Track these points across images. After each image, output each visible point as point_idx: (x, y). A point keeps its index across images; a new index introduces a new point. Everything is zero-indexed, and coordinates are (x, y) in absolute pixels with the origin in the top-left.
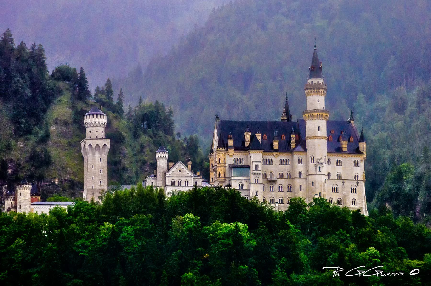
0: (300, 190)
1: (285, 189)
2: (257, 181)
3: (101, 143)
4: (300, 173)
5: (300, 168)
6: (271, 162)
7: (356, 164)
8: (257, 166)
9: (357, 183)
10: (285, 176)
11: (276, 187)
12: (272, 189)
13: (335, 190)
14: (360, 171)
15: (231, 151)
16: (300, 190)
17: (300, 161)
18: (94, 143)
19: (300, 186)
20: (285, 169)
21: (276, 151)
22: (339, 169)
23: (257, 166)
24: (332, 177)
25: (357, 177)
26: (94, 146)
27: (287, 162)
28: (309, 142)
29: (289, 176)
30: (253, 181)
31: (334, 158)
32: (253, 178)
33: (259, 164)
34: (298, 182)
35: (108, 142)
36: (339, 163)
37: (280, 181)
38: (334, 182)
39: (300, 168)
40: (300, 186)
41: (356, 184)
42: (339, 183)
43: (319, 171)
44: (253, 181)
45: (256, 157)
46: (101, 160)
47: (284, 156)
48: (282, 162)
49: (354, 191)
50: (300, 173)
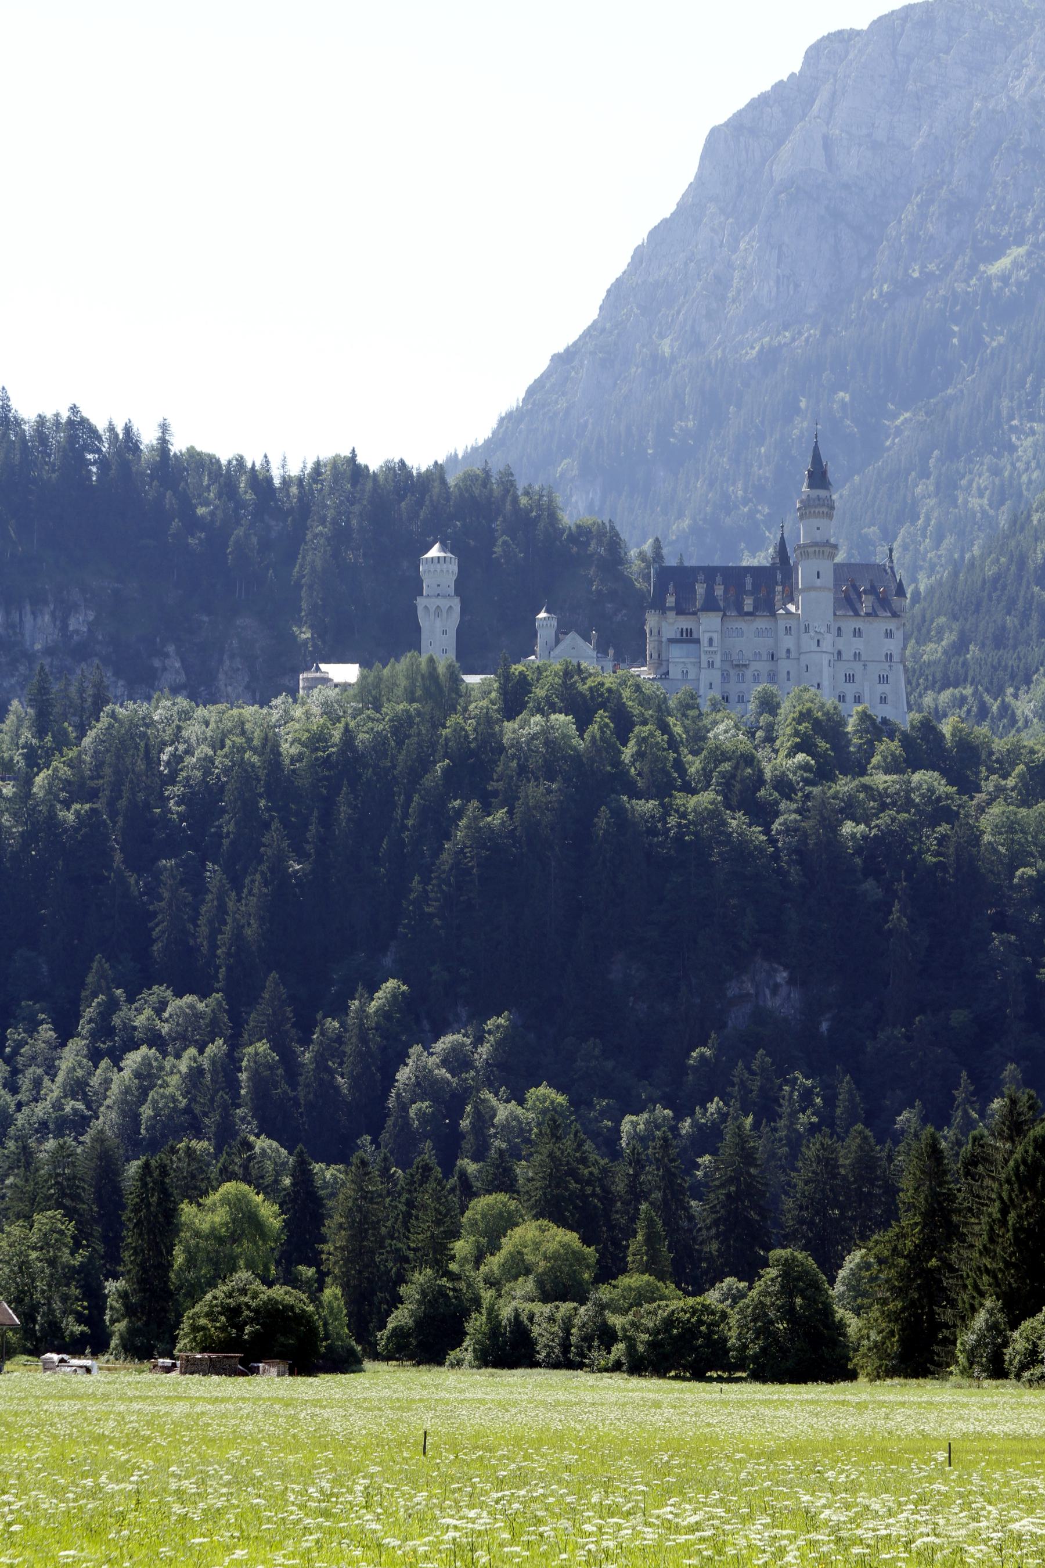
0: (788, 680)
3: (444, 603)
4: (788, 651)
7: (889, 634)
8: (711, 640)
9: (890, 666)
11: (748, 674)
12: (741, 679)
13: (850, 678)
15: (671, 615)
16: (788, 680)
18: (433, 603)
19: (788, 673)
22: (858, 644)
23: (711, 640)
24: (844, 657)
26: (432, 610)
30: (704, 664)
31: (850, 624)
32: (704, 658)
34: (784, 665)
35: (456, 603)
36: (857, 633)
40: (788, 673)
41: (888, 669)
42: (858, 667)
43: (818, 645)
44: (704, 664)
45: (709, 625)
46: (444, 632)
49: (883, 679)
50: (788, 651)
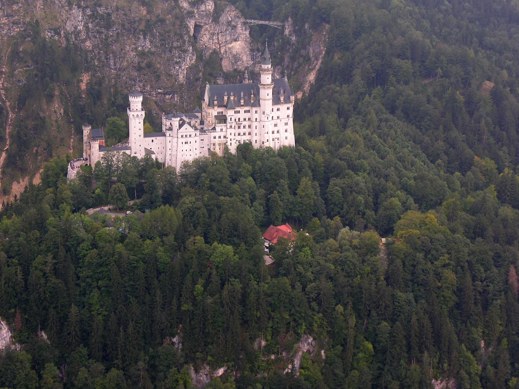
1: (247, 127)
2: (231, 127)
5: (256, 116)
6: (239, 112)
7: (288, 109)
10: (247, 119)
11: (242, 127)
12: (239, 127)
13: (276, 125)
14: (291, 112)
17: (256, 112)
20: (247, 116)
21: (242, 106)
22: (278, 113)
25: (288, 116)
27: (249, 111)
28: (261, 102)
29: (249, 119)
31: (276, 107)
33: (232, 117)
34: (254, 124)
36: (278, 110)
37: (244, 123)
38: (275, 121)
39: (256, 116)
47: (247, 108)
48: (245, 112)
49: (286, 124)
